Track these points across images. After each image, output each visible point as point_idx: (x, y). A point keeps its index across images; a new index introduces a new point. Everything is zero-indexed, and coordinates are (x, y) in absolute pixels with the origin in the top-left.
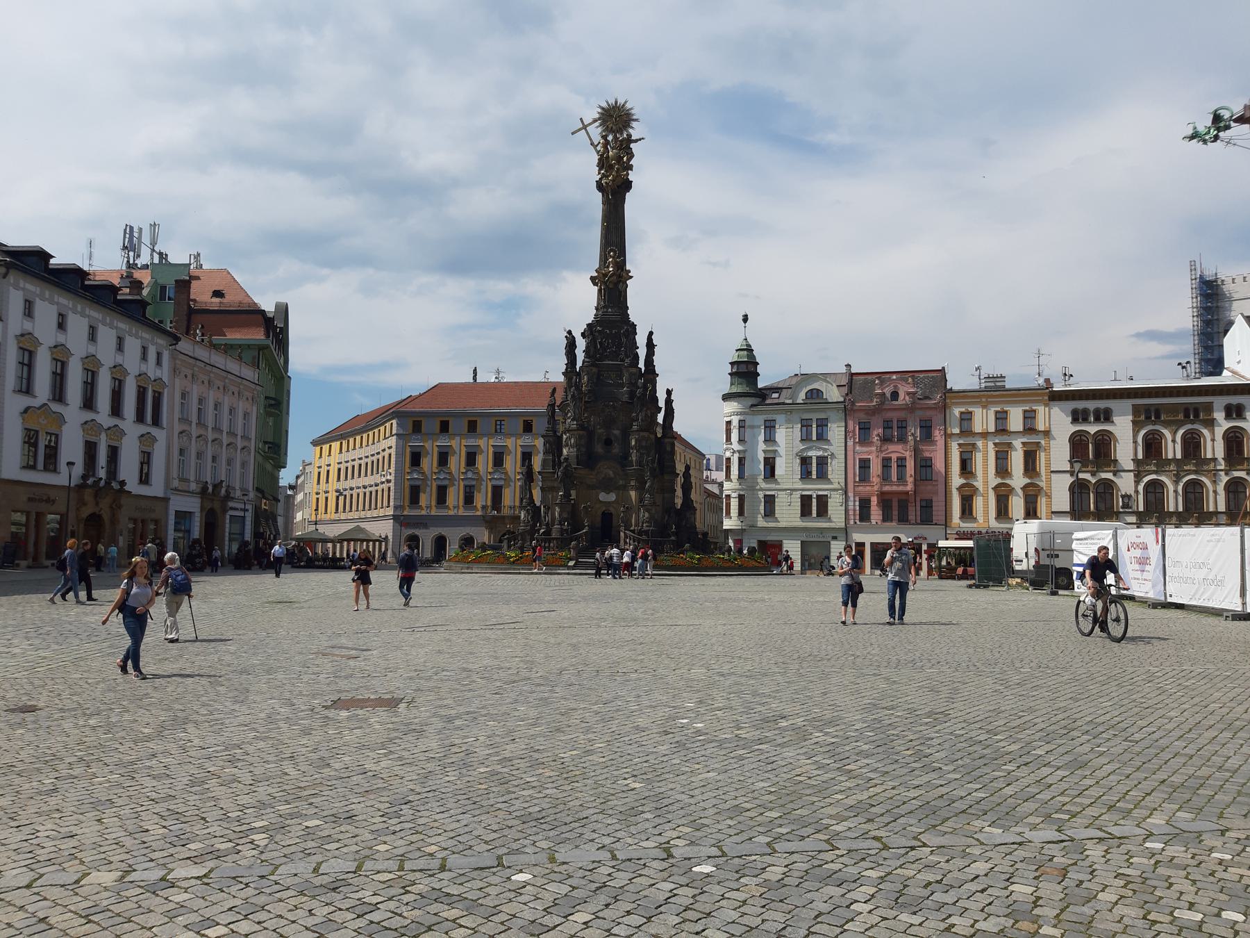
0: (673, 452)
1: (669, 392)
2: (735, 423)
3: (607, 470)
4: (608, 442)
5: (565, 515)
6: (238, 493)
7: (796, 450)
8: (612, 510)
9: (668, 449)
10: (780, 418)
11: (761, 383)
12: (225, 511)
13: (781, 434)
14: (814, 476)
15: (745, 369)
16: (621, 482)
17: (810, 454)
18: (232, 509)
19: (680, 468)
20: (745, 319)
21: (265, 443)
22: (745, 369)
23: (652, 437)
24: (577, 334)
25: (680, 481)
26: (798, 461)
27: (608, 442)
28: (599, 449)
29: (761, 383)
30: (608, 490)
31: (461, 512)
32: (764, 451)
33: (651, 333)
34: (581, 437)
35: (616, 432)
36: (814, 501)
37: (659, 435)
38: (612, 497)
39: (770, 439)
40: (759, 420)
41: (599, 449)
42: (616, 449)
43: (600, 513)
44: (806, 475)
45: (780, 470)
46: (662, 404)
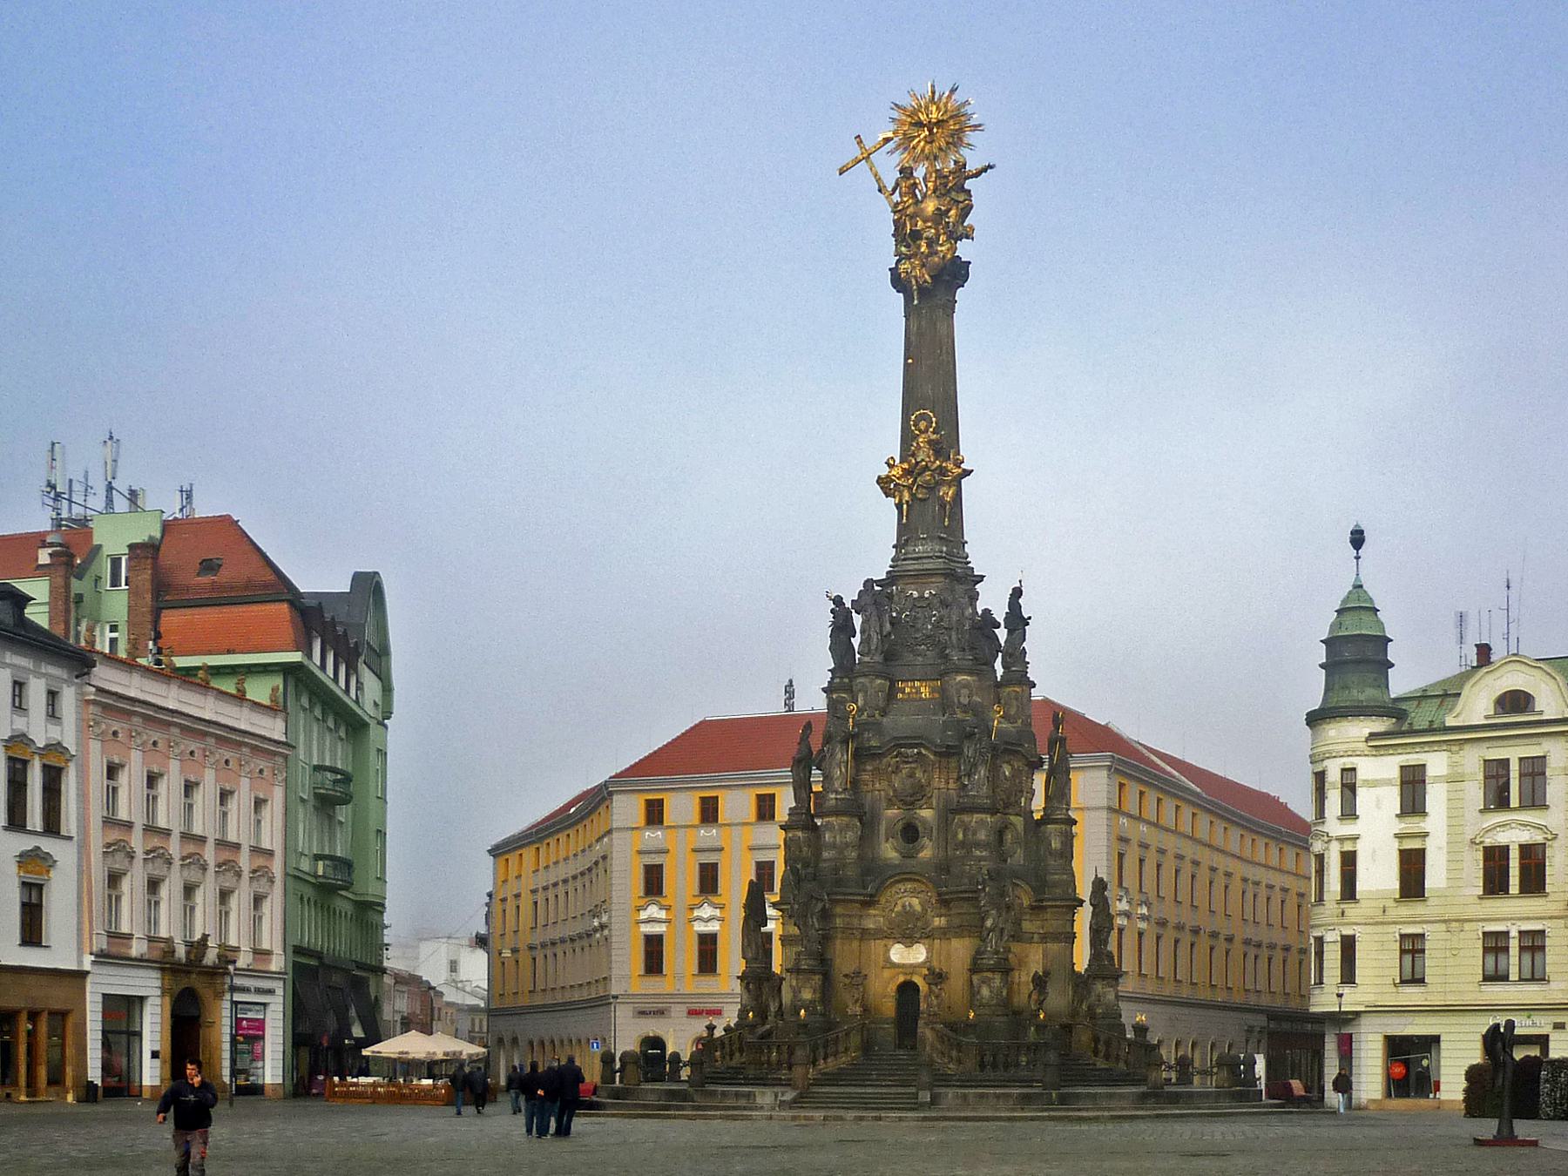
0: (1067, 853)
2: (1334, 776)
3: (908, 898)
4: (910, 833)
5: (807, 995)
6: (243, 961)
8: (918, 980)
9: (1056, 844)
10: (1436, 764)
11: (1400, 683)
12: (219, 995)
13: (1436, 797)
14: (1514, 888)
15: (1356, 655)
16: (938, 922)
17: (1502, 838)
18: (233, 989)
19: (1084, 890)
21: (318, 857)
22: (1356, 655)
23: (1018, 821)
24: (848, 605)
25: (1083, 919)
26: (1480, 856)
27: (910, 833)
28: (889, 851)
29: (1400, 683)
30: (908, 939)
32: (1400, 837)
34: (844, 829)
35: (926, 813)
36: (1514, 945)
38: (918, 954)
41: (889, 851)
42: (927, 852)
43: (892, 988)
44: (1495, 884)
45: (1435, 876)
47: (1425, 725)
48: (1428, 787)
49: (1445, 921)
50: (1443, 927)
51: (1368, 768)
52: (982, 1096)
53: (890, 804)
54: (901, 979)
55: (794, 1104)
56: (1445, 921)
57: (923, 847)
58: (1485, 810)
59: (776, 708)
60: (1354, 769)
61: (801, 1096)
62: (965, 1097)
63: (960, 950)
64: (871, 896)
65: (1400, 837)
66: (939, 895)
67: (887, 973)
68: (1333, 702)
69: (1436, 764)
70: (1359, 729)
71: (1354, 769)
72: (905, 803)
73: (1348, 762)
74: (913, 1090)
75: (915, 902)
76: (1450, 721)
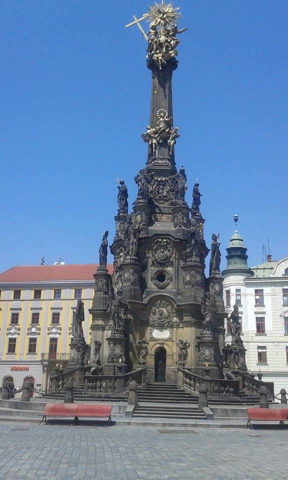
1: (215, 238)
4: (161, 277)
7: (280, 312)
8: (165, 347)
10: (267, 290)
13: (267, 300)
20: (236, 220)
30: (161, 327)
31: (26, 357)
33: (197, 185)
37: (207, 276)
38: (166, 334)
39: (259, 303)
40: (252, 290)
45: (268, 326)
46: (209, 246)
47: (262, 277)
48: (265, 297)
49: (273, 342)
50: (272, 344)
51: (244, 289)
52: (235, 411)
53: (153, 264)
54: (158, 346)
55: (133, 414)
56: (273, 342)
57: (168, 284)
58: (283, 306)
59: (38, 264)
60: (240, 290)
61: (135, 409)
62: (226, 410)
63: (188, 334)
64: (146, 305)
65: (256, 313)
66: (178, 306)
67: (151, 343)
68: (231, 267)
69: (267, 290)
70: (240, 278)
71: (240, 290)
72: (160, 263)
73: (238, 287)
74: (196, 406)
75: (165, 310)
76: (271, 276)
